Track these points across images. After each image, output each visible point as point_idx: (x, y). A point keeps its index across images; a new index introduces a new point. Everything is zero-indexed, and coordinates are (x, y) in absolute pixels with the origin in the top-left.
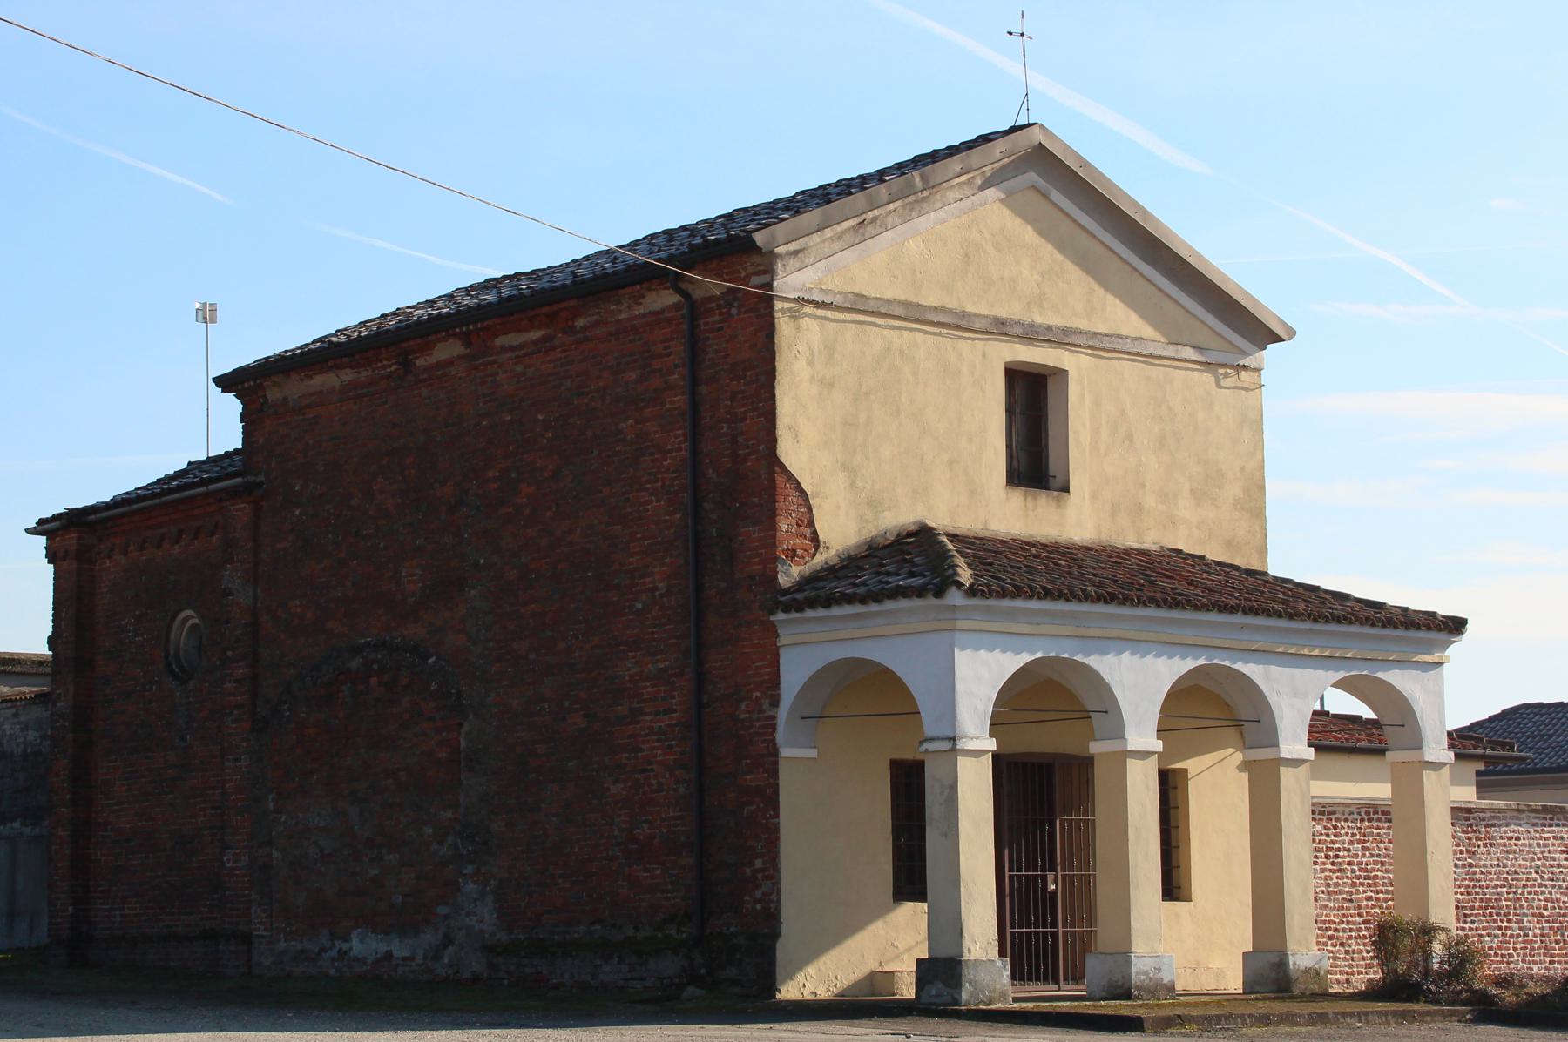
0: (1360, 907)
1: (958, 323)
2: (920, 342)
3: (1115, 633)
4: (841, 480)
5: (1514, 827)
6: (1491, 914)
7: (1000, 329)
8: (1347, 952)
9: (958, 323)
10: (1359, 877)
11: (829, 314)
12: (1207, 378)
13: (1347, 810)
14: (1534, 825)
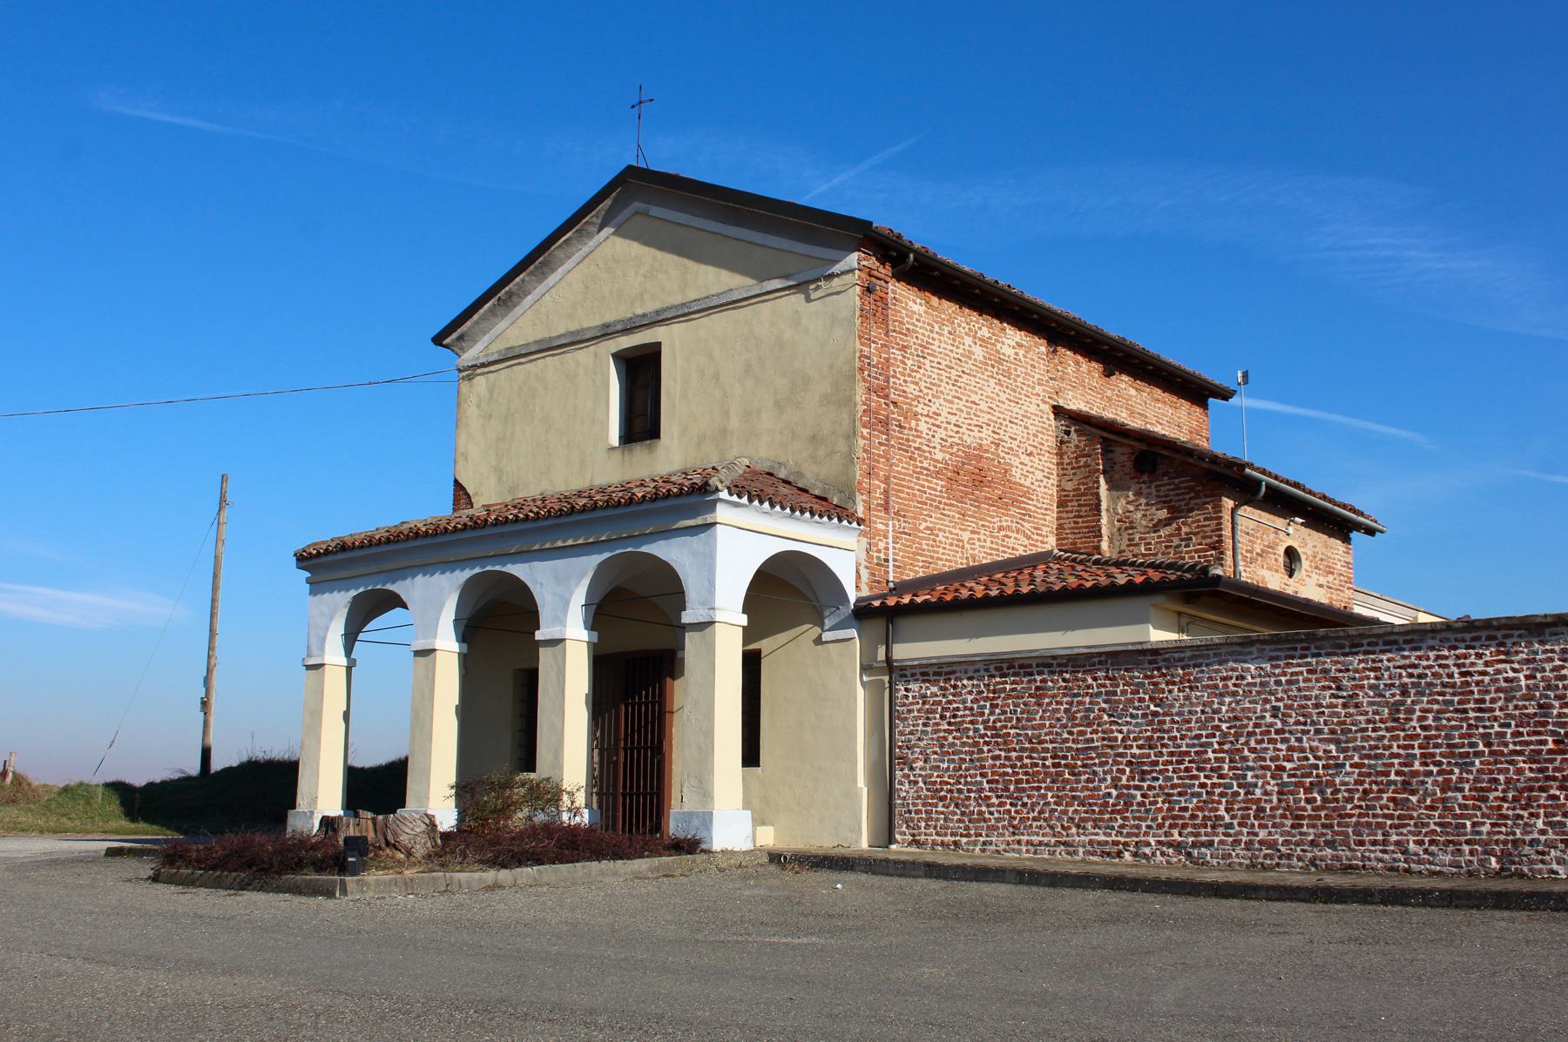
0: (983, 767)
1: (576, 341)
2: (550, 363)
3: (405, 564)
4: (493, 479)
5: (1231, 664)
6: (1187, 770)
7: (606, 332)
8: (963, 814)
9: (576, 341)
10: (982, 736)
11: (492, 368)
12: (797, 299)
13: (972, 668)
14: (1271, 659)
